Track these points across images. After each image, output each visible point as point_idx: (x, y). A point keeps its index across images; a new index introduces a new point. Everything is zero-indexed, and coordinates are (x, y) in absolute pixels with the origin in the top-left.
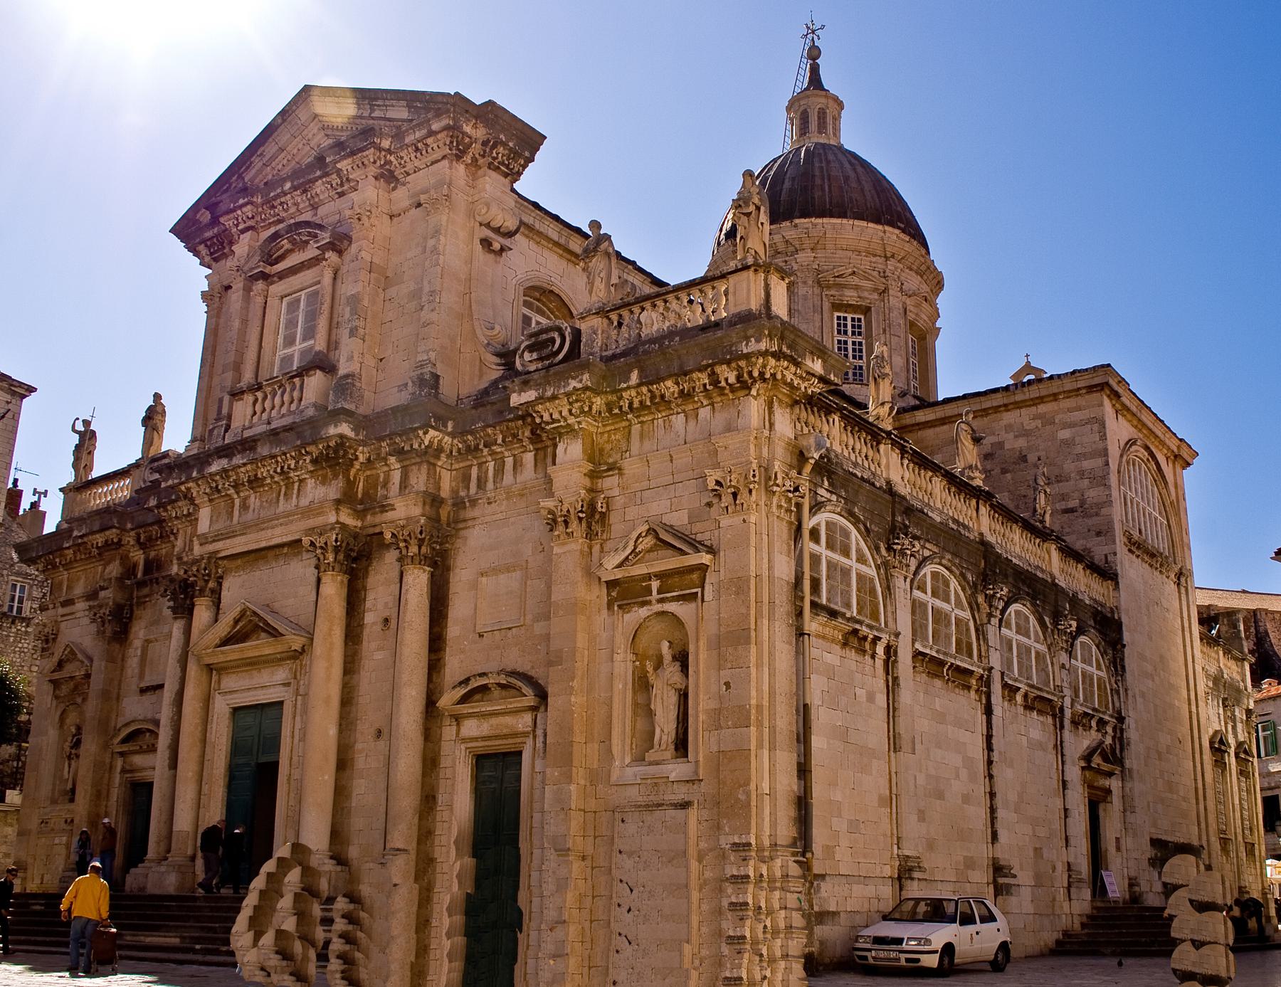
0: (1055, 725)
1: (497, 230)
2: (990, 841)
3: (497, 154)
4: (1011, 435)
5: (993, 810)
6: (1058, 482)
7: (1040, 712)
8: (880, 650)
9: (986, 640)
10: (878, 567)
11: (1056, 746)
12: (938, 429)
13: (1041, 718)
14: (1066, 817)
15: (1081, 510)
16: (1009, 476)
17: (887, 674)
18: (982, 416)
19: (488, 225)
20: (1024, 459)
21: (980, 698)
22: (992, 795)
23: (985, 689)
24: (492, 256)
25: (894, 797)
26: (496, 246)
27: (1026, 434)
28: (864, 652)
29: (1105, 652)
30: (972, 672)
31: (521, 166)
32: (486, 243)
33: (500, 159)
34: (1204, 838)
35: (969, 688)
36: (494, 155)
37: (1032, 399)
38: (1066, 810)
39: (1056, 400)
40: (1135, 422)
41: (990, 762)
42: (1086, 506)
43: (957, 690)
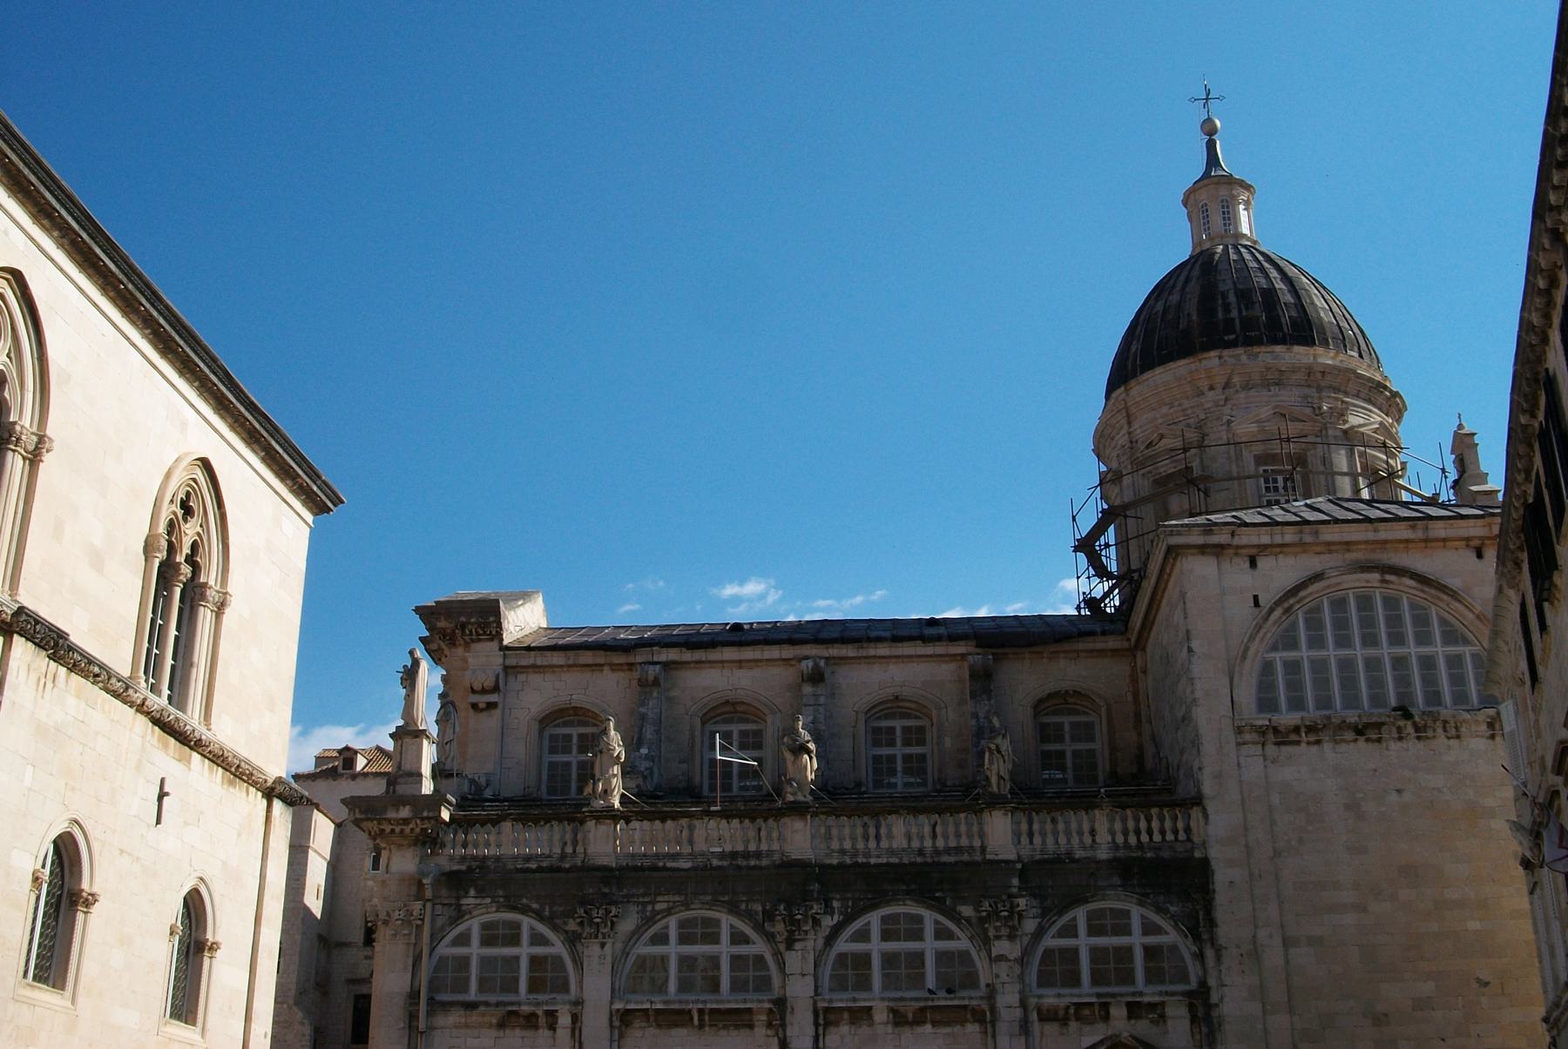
1: (484, 691)
3: (471, 631)
7: (935, 1024)
8: (564, 1020)
19: (473, 691)
24: (485, 713)
26: (482, 706)
28: (536, 1027)
30: (749, 1010)
31: (497, 627)
32: (474, 706)
33: (474, 633)
35: (751, 1027)
36: (467, 632)
43: (723, 1032)
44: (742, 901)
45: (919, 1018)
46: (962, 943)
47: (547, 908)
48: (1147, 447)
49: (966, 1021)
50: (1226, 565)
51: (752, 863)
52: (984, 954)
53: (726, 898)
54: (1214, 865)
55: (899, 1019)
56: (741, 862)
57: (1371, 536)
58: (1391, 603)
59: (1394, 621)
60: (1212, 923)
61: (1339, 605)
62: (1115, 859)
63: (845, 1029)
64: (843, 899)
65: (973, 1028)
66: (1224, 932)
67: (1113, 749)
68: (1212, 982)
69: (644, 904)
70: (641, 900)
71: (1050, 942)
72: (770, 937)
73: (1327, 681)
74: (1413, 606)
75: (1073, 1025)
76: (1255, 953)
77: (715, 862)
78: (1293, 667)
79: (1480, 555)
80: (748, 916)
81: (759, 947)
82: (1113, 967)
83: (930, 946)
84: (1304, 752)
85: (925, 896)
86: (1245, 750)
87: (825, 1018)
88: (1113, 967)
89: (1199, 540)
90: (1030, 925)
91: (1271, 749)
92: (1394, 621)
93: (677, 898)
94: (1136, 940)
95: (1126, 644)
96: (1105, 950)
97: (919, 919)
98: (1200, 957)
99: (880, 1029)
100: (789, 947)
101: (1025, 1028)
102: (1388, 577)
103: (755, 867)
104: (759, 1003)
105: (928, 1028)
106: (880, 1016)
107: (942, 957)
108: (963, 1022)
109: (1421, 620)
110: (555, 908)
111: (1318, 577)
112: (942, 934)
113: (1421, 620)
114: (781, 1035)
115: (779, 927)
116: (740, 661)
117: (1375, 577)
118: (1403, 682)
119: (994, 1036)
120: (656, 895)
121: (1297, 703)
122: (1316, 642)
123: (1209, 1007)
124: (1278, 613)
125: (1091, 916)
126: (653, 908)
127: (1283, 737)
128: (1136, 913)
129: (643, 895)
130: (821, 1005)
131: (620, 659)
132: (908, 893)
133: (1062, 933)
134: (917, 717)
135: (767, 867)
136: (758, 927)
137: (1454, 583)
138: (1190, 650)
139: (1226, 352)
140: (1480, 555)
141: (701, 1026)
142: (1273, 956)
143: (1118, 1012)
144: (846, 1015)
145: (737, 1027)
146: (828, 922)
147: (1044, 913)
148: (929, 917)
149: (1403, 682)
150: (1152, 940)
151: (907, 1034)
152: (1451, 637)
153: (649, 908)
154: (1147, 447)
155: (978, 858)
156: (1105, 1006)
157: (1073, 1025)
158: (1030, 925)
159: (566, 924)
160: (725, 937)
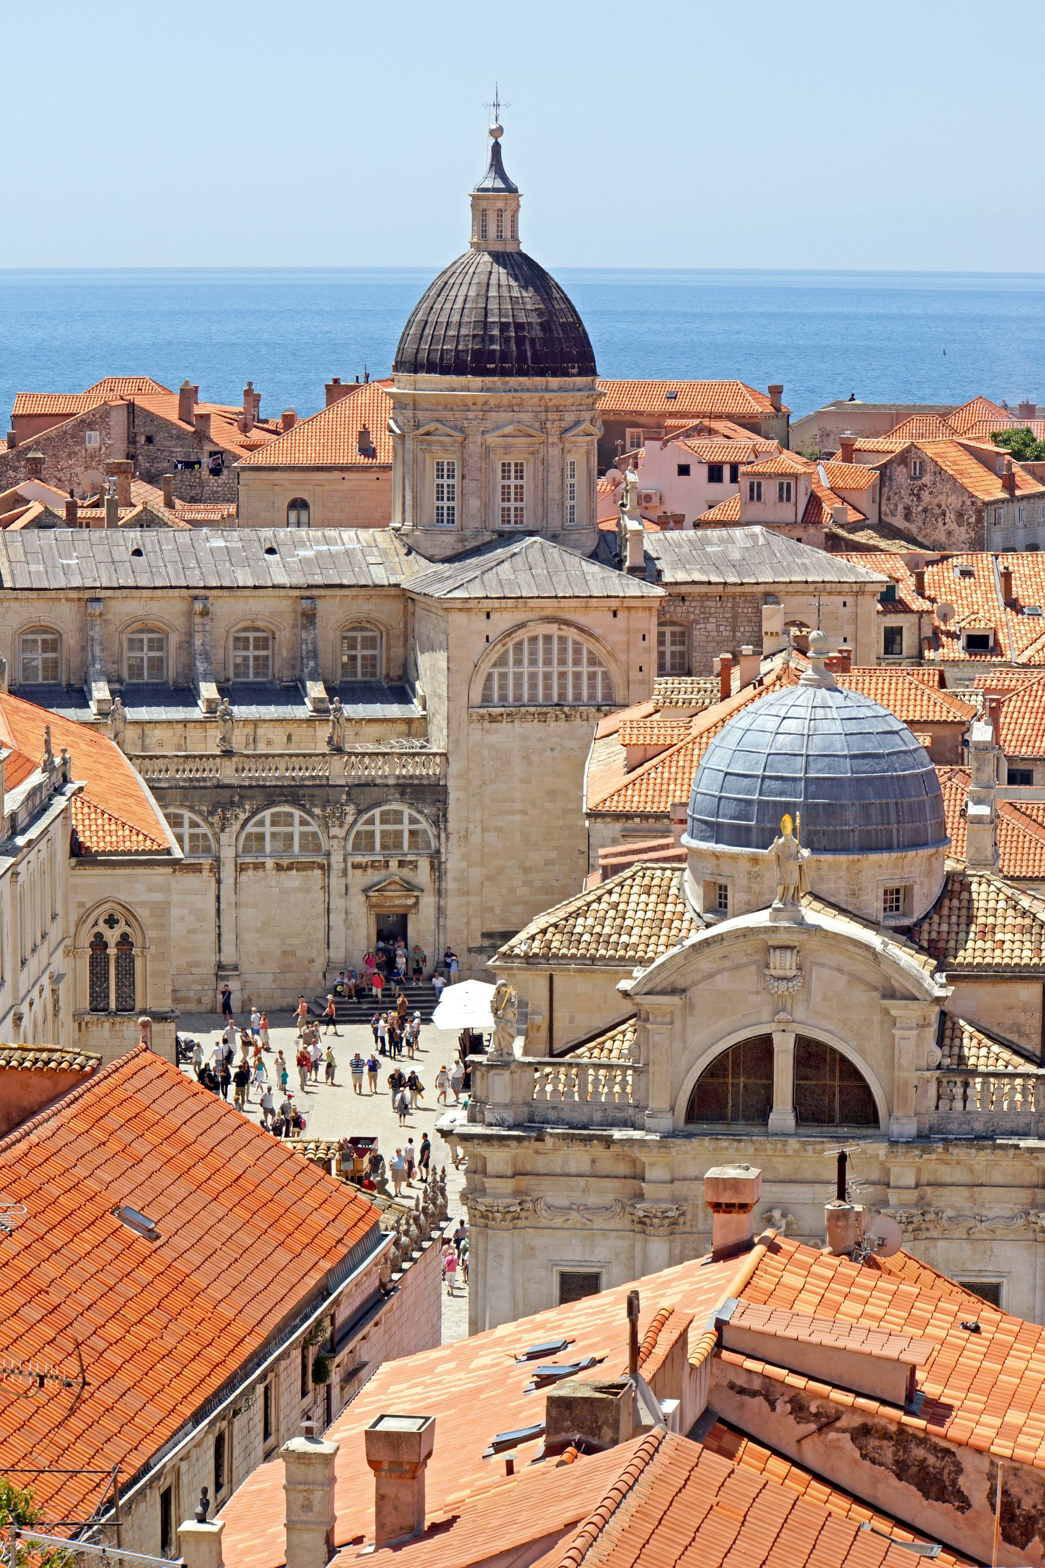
45: (290, 868)
46: (314, 827)
50: (473, 617)
54: (450, 789)
55: (279, 868)
56: (196, 784)
57: (556, 605)
58: (562, 640)
59: (563, 650)
60: (446, 821)
62: (397, 785)
63: (250, 872)
64: (251, 805)
65: (318, 872)
66: (451, 826)
67: (389, 659)
68: (443, 850)
71: (359, 827)
72: (212, 825)
73: (521, 685)
74: (575, 643)
75: (370, 871)
76: (466, 837)
77: (182, 784)
78: (503, 676)
79: (615, 615)
80: (200, 813)
81: (204, 829)
82: (392, 842)
83: (297, 829)
84: (504, 726)
86: (472, 726)
87: (241, 868)
88: (392, 842)
89: (460, 606)
90: (350, 819)
91: (486, 724)
92: (563, 650)
94: (406, 827)
96: (388, 832)
97: (291, 815)
98: (439, 837)
99: (269, 872)
100: (223, 830)
101: (345, 873)
104: (207, 862)
105: (294, 872)
107: (303, 835)
108: (313, 868)
109: (577, 651)
111: (522, 625)
112: (303, 823)
113: (577, 651)
115: (215, 819)
117: (556, 626)
118: (563, 687)
121: (503, 698)
122: (518, 662)
123: (440, 863)
124: (499, 646)
125: (382, 814)
127: (493, 719)
128: (407, 811)
130: (239, 861)
131: (74, 595)
132: (286, 802)
133: (367, 823)
136: (206, 820)
137: (598, 631)
139: (488, 379)
140: (615, 615)
142: (476, 838)
143: (393, 864)
146: (243, 816)
147: (359, 813)
148: (297, 813)
149: (563, 687)
150: (414, 827)
151: (283, 873)
152: (593, 661)
155: (324, 782)
156: (387, 862)
157: (370, 871)
158: (350, 819)
160: (186, 824)
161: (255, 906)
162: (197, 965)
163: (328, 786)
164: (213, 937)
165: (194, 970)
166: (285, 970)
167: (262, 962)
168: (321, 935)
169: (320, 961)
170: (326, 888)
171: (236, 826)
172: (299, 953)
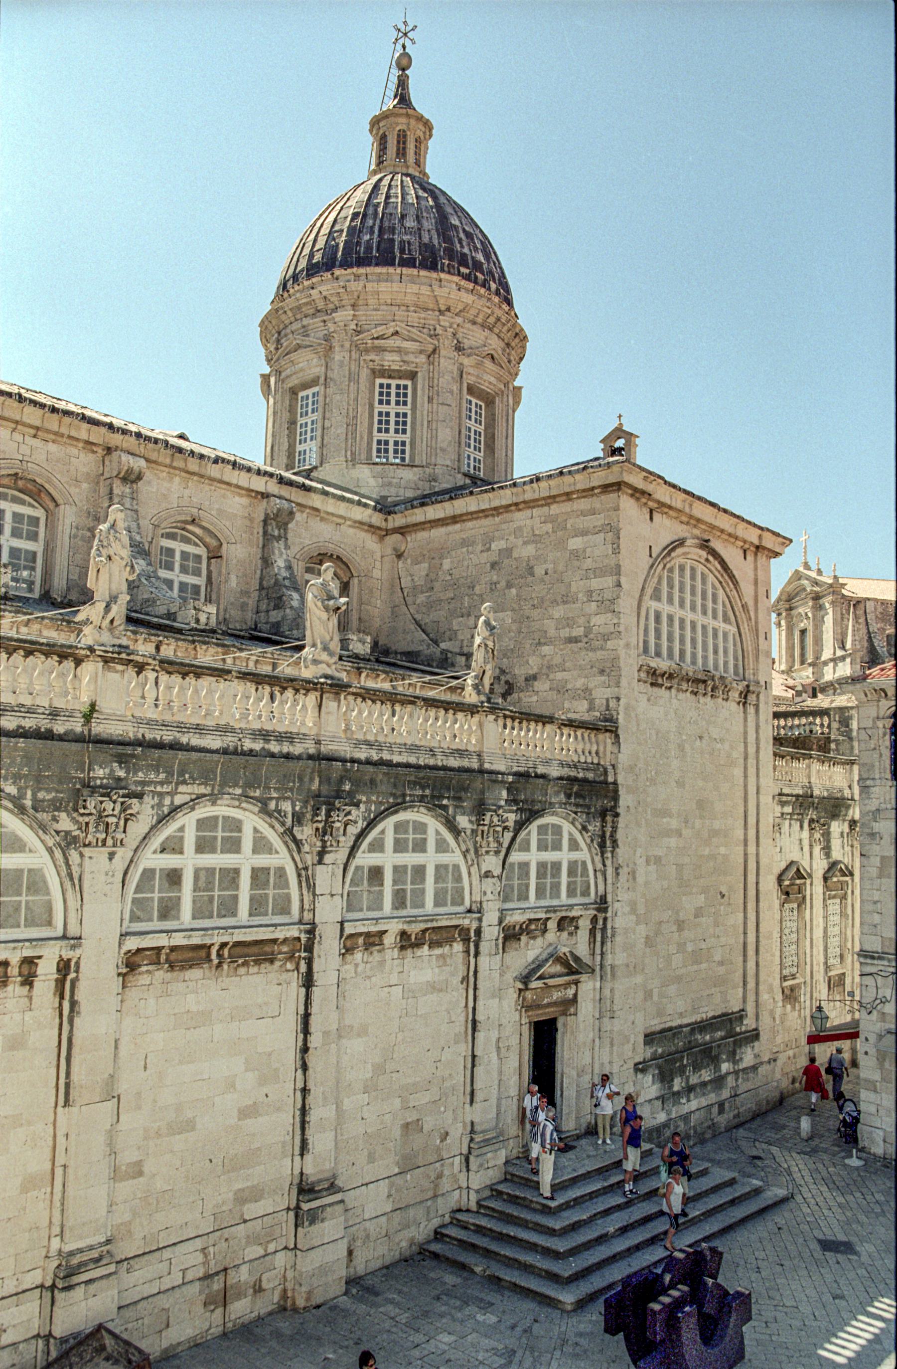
0: (467, 952)
2: (297, 1151)
4: (520, 542)
5: (304, 1111)
6: (565, 603)
8: (47, 969)
9: (312, 887)
10: (50, 851)
11: (465, 979)
12: (450, 528)
13: (438, 951)
14: (473, 1066)
15: (585, 640)
16: (514, 591)
17: (62, 997)
18: (493, 515)
20: (530, 571)
21: (298, 965)
22: (305, 1091)
23: (303, 955)
25: (59, 1172)
27: (536, 539)
29: (584, 828)
34: (751, 998)
37: (544, 498)
38: (474, 1057)
39: (570, 500)
40: (684, 519)
41: (305, 1049)
42: (591, 636)
43: (242, 970)
44: (271, 799)
47: (29, 793)
48: (377, 338)
49: (454, 940)
51: (286, 748)
52: (474, 870)
53: (257, 793)
60: (615, 843)
61: (682, 568)
69: (161, 795)
70: (159, 789)
85: (434, 804)
93: (202, 790)
95: (383, 525)
102: (711, 558)
103: (288, 756)
105: (426, 947)
106: (389, 940)
108: (450, 941)
110: (41, 795)
114: (303, 967)
115: (305, 832)
116: (38, 429)
119: (477, 954)
120: (178, 784)
126: (172, 802)
129: (162, 783)
132: (422, 798)
134: (196, 545)
135: (299, 758)
138: (619, 585)
141: (219, 965)
144: (361, 941)
145: (258, 962)
153: (167, 801)
154: (377, 338)
157: (524, 938)
159: (55, 819)
160: (247, 843)
161: (363, 1031)
162: (254, 1194)
163: (481, 771)
164: (288, 1118)
165: (252, 1210)
166: (407, 1166)
167: (371, 1158)
168: (460, 1078)
169: (458, 1132)
170: (471, 980)
171: (341, 855)
172: (429, 1123)
